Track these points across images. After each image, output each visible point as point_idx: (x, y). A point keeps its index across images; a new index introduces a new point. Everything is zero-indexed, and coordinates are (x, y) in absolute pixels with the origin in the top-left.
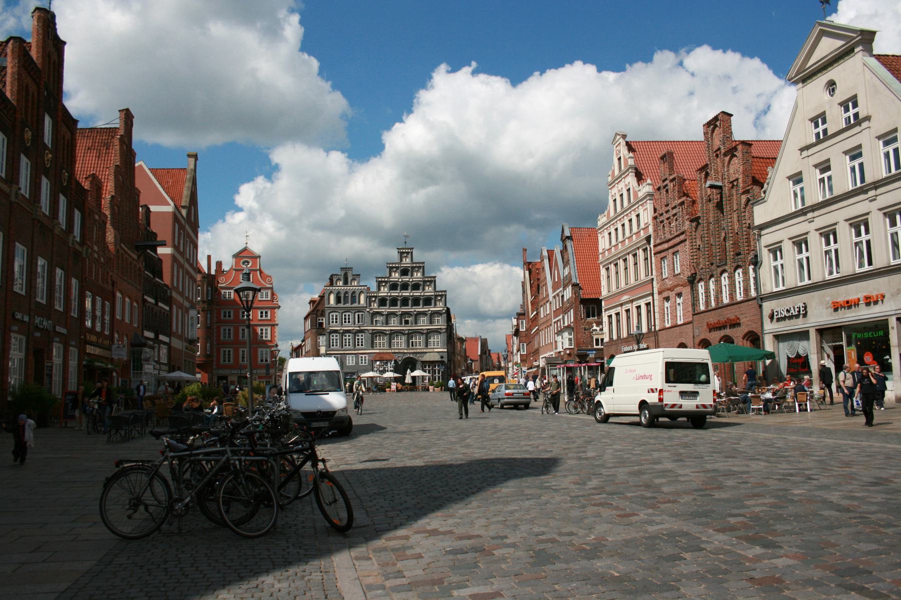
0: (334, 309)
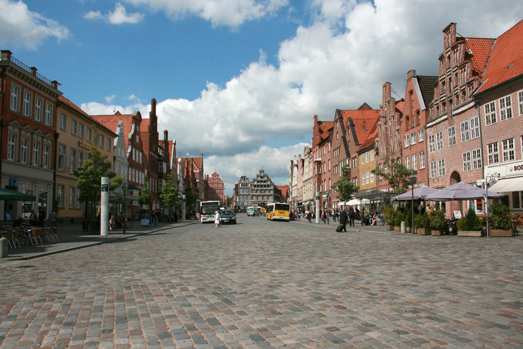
0: (241, 188)
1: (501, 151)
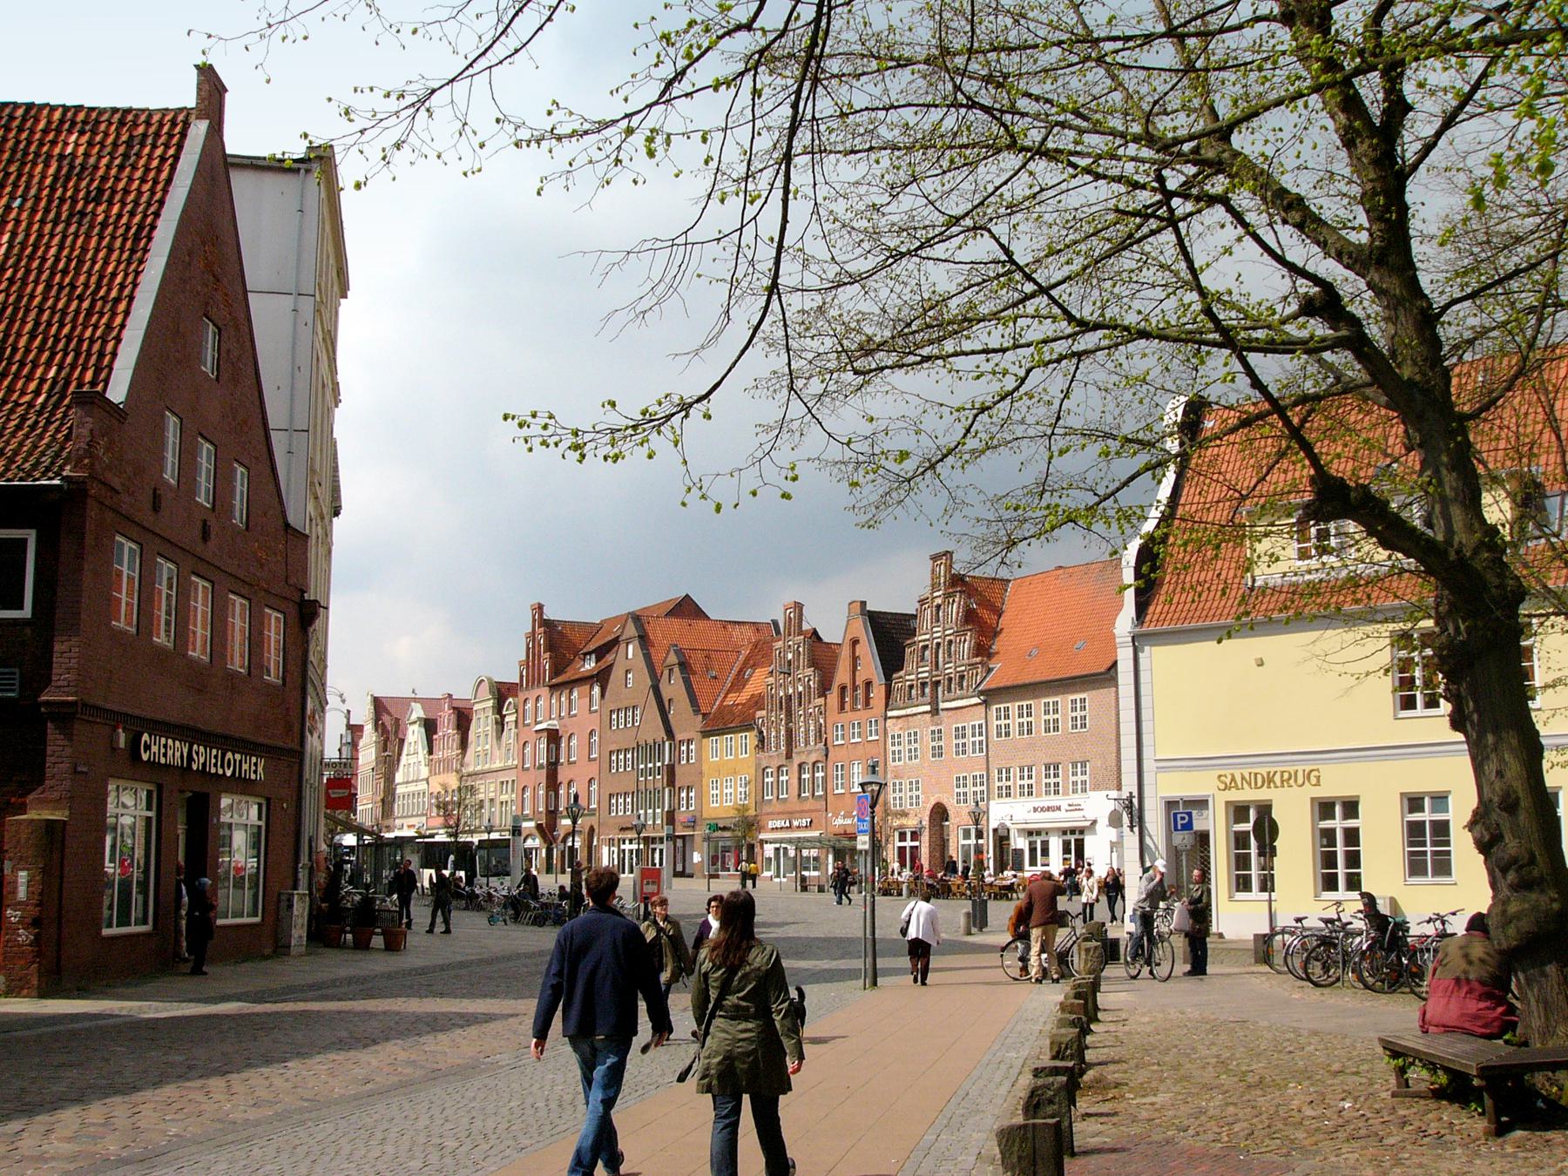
1: (1016, 782)
